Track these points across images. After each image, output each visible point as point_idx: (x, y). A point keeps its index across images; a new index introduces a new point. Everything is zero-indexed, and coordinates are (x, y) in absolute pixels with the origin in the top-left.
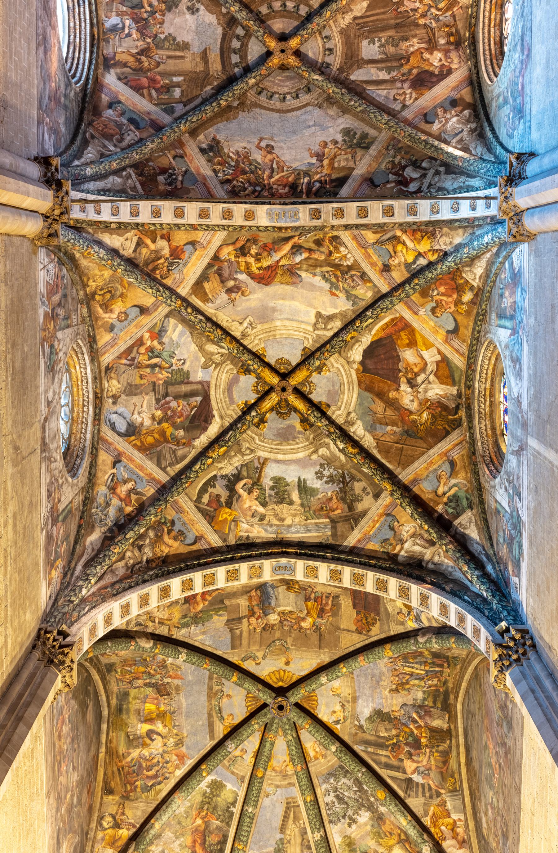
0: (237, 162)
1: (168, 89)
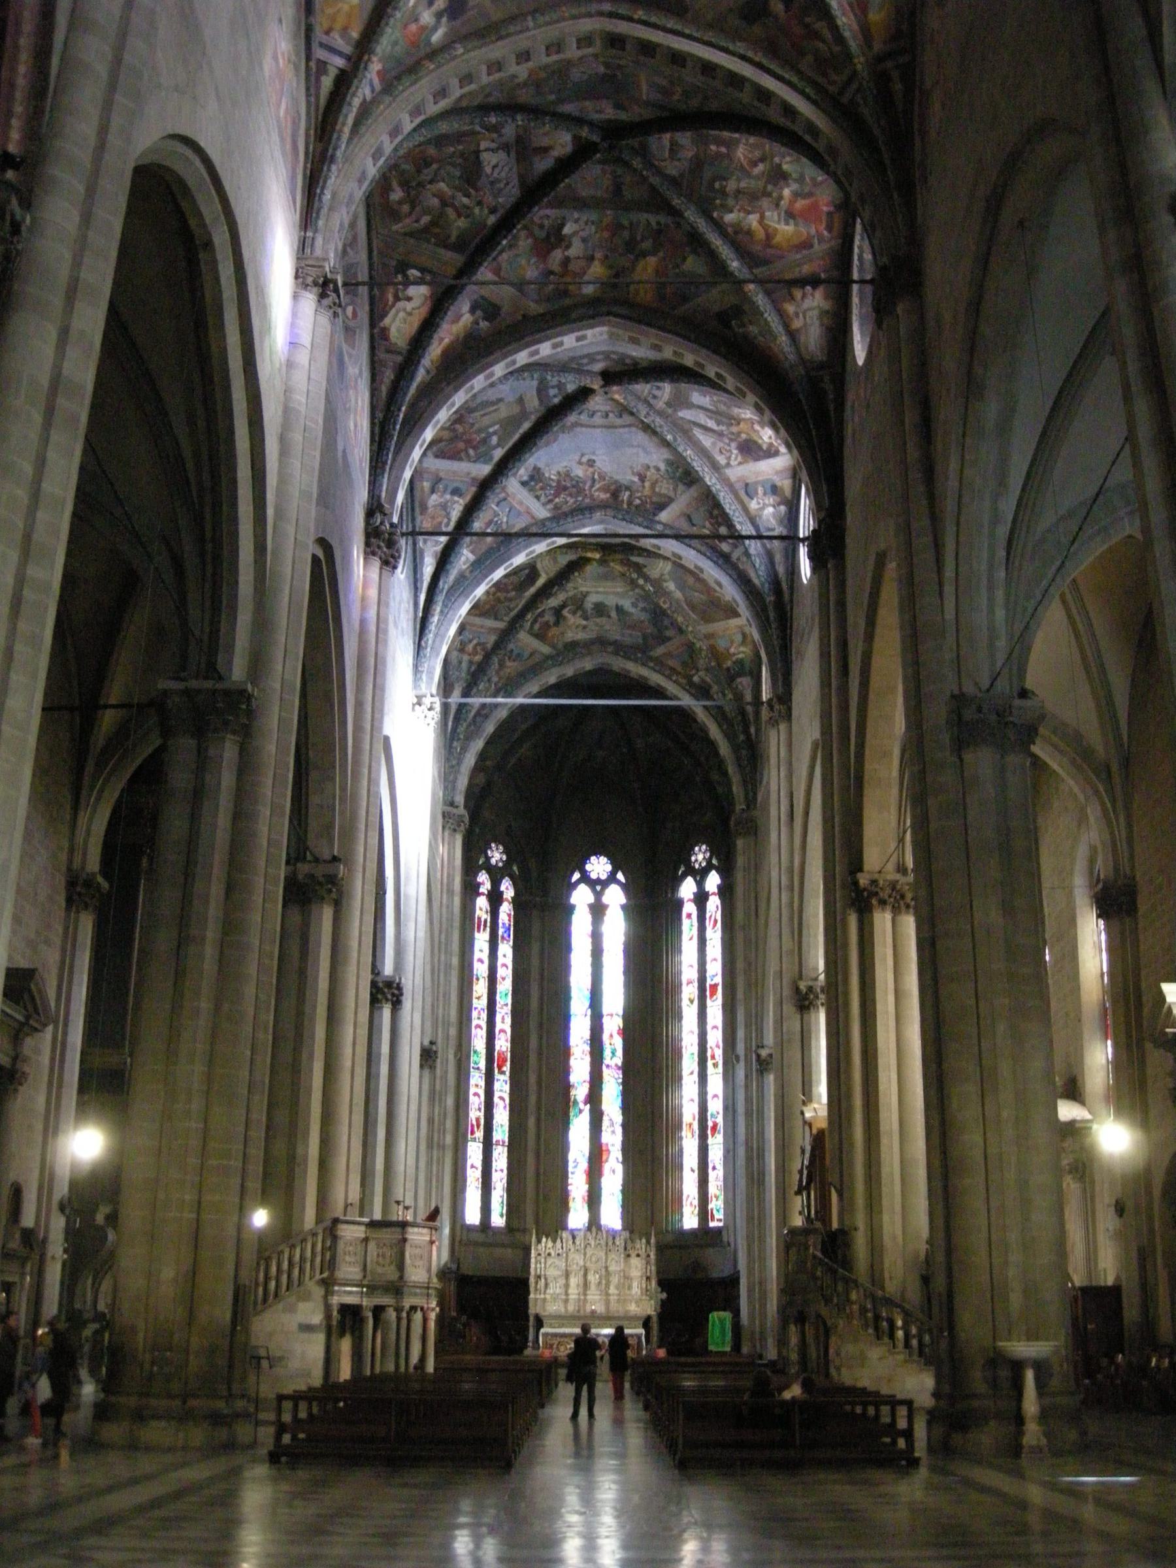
0: (559, 482)
1: (484, 441)
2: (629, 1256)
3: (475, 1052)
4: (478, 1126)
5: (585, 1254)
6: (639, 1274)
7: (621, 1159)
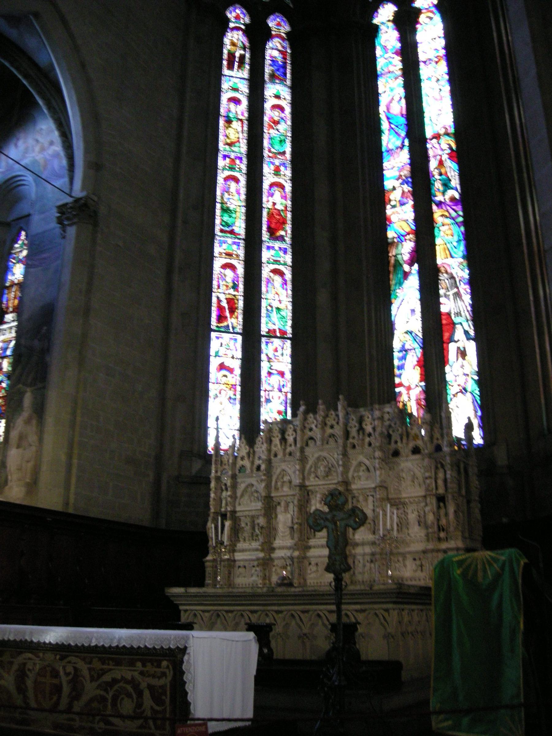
2: (396, 454)
3: (226, 210)
4: (232, 310)
5: (303, 460)
6: (421, 492)
7: (472, 333)
